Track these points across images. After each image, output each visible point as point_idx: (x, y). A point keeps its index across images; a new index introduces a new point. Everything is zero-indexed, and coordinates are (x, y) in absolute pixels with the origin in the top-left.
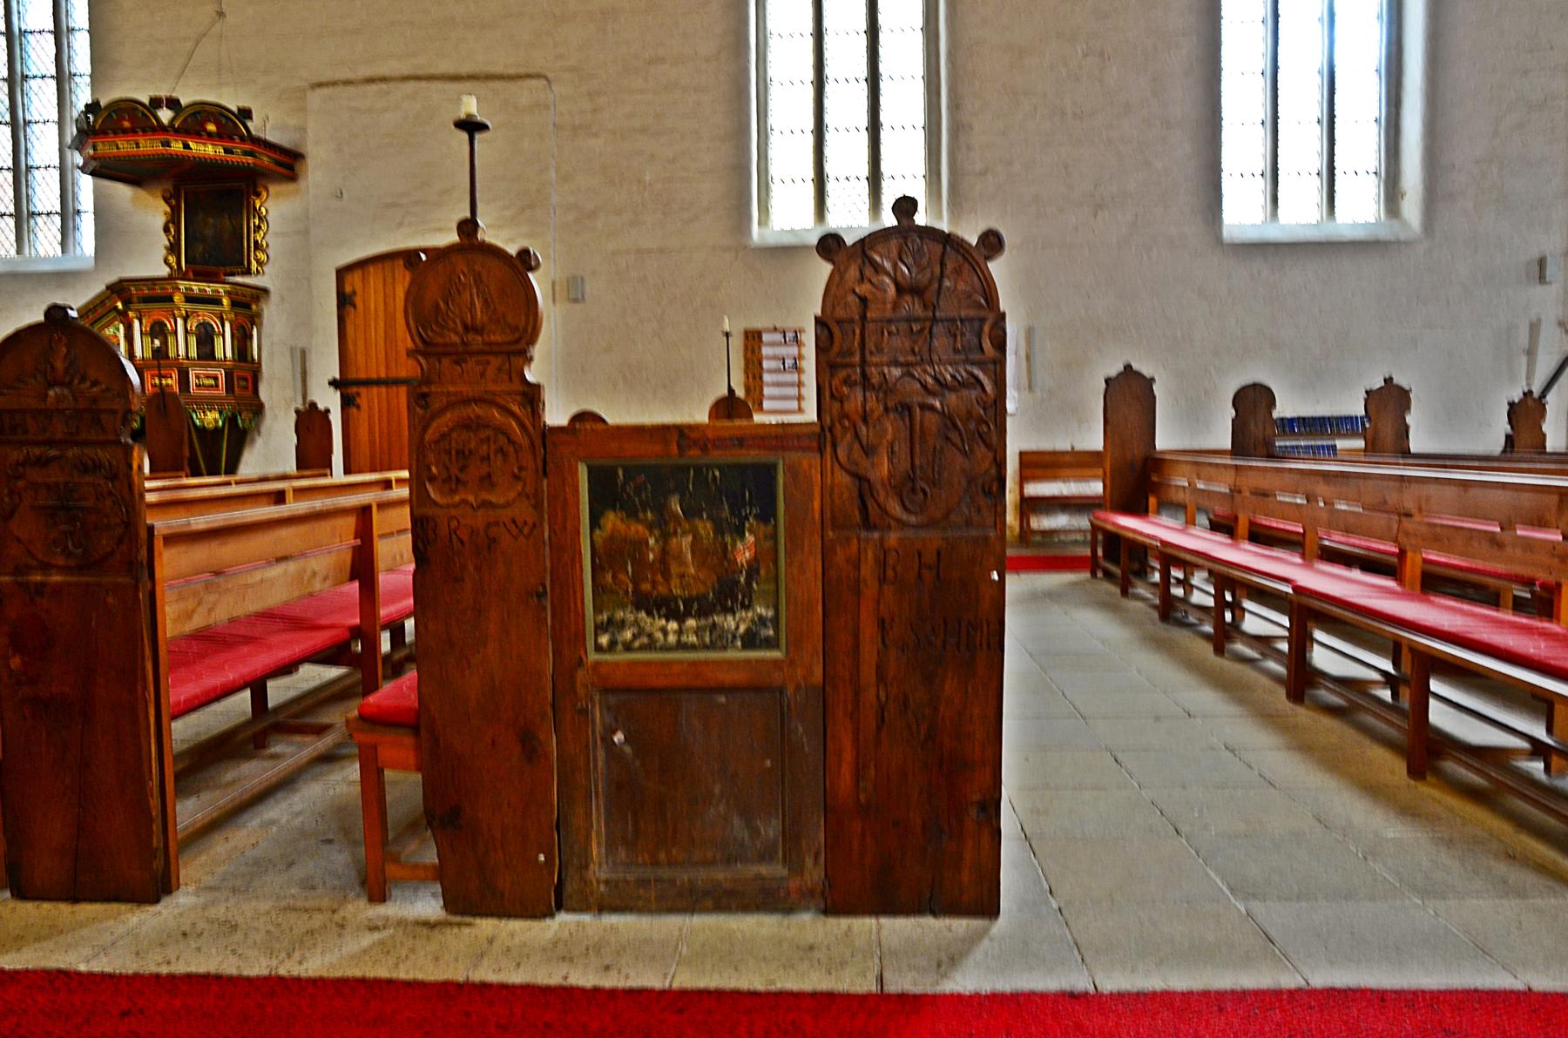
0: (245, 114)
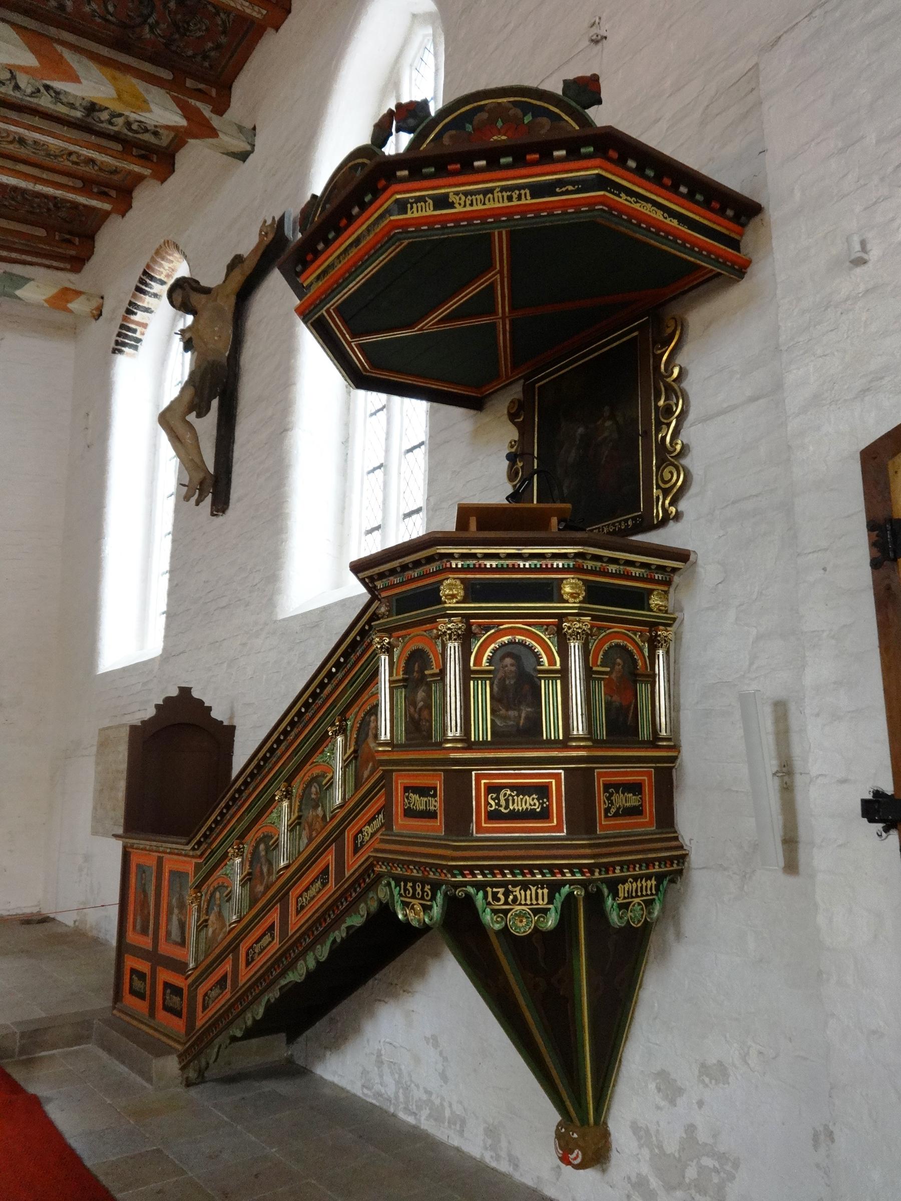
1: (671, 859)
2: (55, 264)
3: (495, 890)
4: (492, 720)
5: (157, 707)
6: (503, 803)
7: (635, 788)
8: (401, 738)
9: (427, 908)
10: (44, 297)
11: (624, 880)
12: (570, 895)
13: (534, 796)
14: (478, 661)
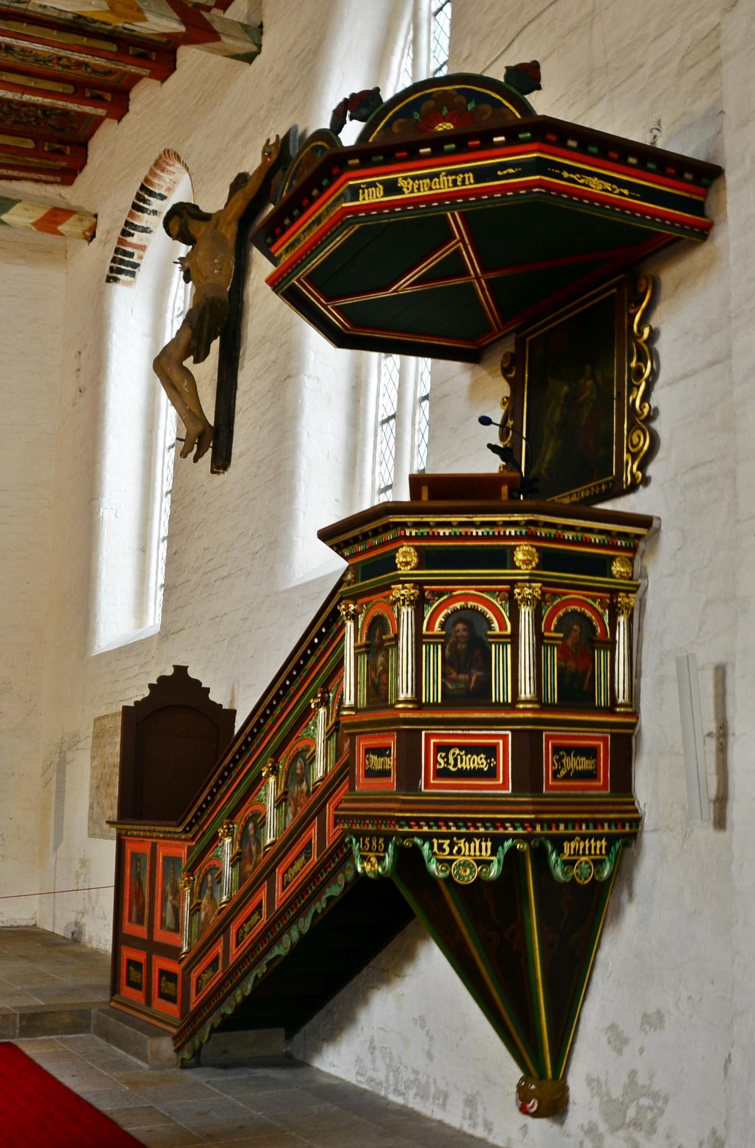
0: (527, 77)
1: (622, 822)
2: (43, 177)
3: (440, 841)
4: (443, 684)
5: (151, 686)
6: (451, 761)
7: (590, 752)
8: (363, 702)
9: (380, 860)
10: (32, 221)
11: (570, 838)
12: (513, 848)
13: (482, 756)
14: (430, 626)
